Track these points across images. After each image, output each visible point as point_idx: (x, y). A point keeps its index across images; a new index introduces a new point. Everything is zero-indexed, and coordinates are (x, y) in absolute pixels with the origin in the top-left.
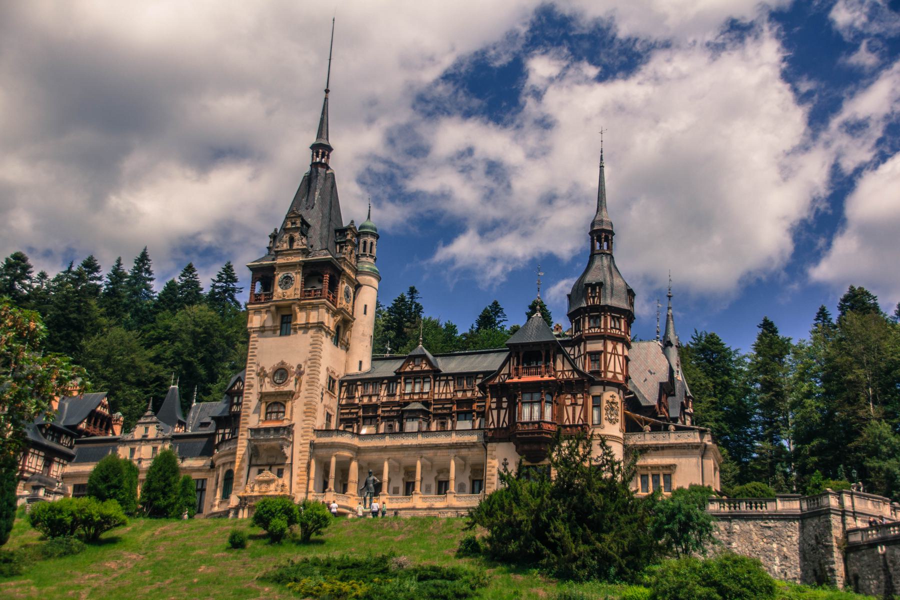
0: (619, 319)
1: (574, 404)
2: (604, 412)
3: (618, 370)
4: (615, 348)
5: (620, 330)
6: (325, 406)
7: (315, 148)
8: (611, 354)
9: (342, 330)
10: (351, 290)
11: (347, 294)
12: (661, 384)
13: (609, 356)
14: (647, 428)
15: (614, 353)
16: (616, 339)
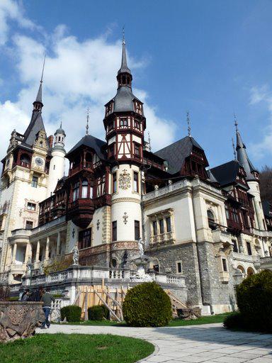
0: (126, 119)
1: (101, 184)
2: (118, 182)
3: (127, 151)
4: (124, 138)
5: (127, 126)
6: (24, 218)
7: (34, 104)
8: (121, 142)
9: (39, 179)
10: (43, 160)
11: (39, 162)
12: (187, 159)
13: (119, 144)
14: (156, 187)
15: (124, 141)
16: (124, 132)
